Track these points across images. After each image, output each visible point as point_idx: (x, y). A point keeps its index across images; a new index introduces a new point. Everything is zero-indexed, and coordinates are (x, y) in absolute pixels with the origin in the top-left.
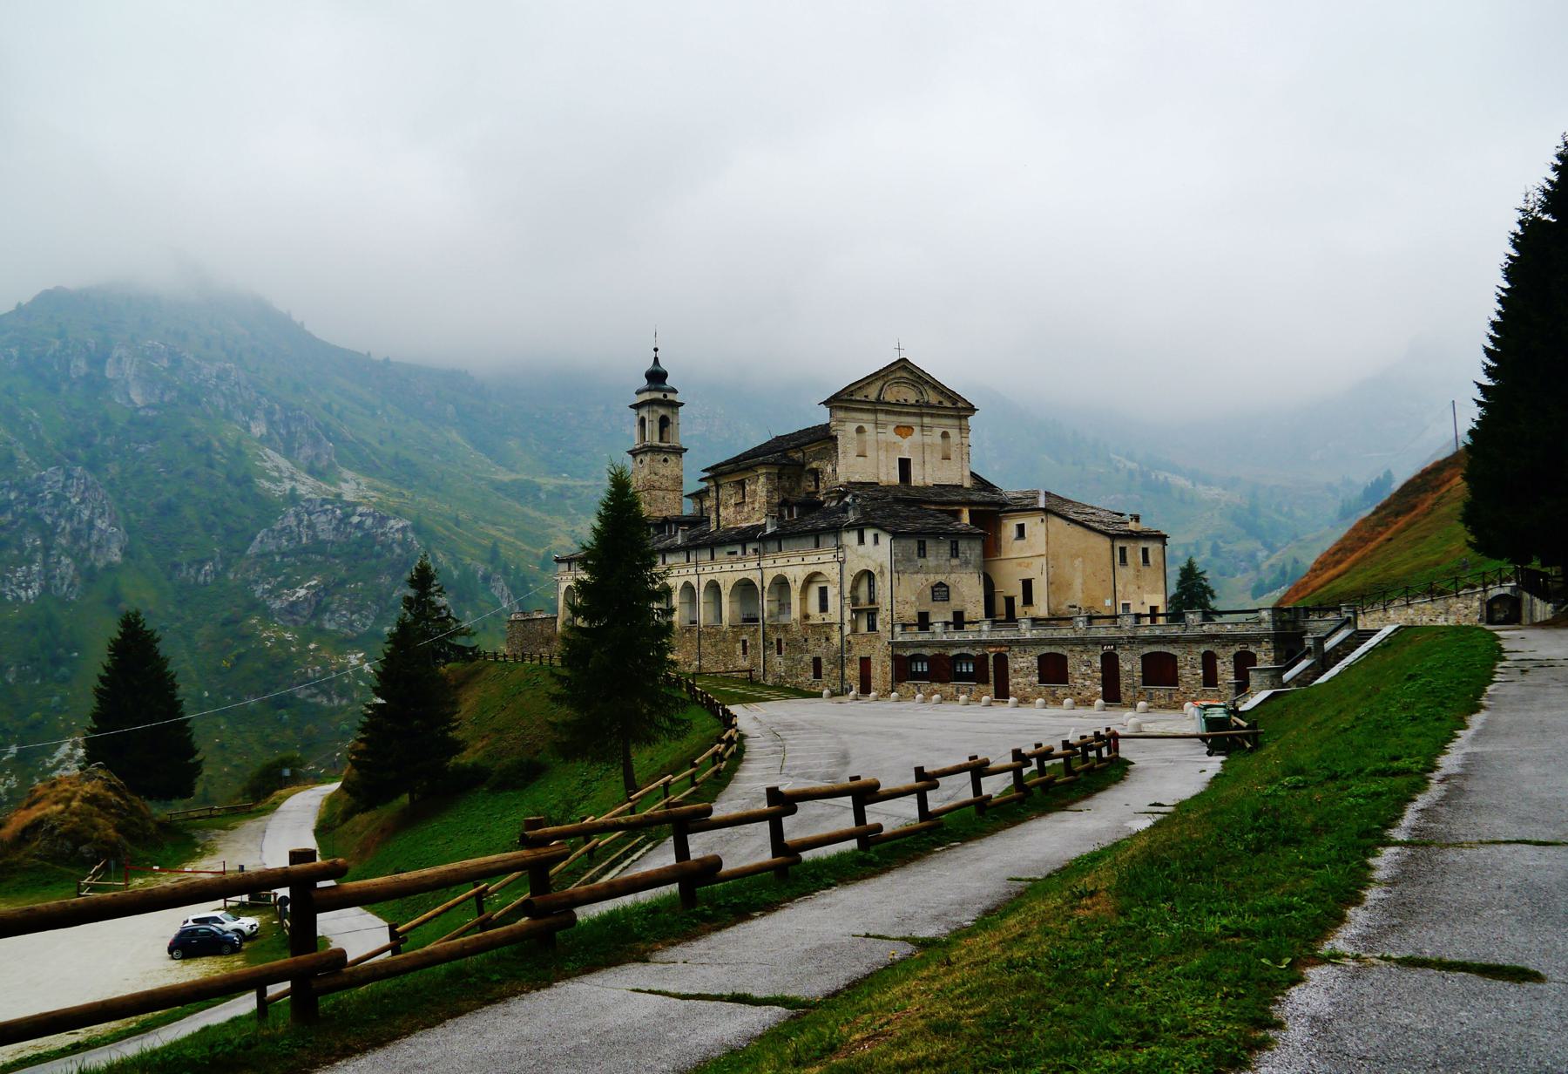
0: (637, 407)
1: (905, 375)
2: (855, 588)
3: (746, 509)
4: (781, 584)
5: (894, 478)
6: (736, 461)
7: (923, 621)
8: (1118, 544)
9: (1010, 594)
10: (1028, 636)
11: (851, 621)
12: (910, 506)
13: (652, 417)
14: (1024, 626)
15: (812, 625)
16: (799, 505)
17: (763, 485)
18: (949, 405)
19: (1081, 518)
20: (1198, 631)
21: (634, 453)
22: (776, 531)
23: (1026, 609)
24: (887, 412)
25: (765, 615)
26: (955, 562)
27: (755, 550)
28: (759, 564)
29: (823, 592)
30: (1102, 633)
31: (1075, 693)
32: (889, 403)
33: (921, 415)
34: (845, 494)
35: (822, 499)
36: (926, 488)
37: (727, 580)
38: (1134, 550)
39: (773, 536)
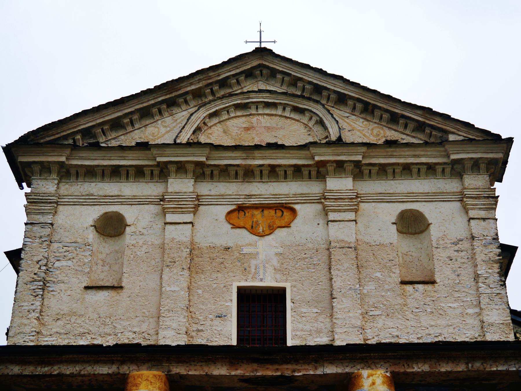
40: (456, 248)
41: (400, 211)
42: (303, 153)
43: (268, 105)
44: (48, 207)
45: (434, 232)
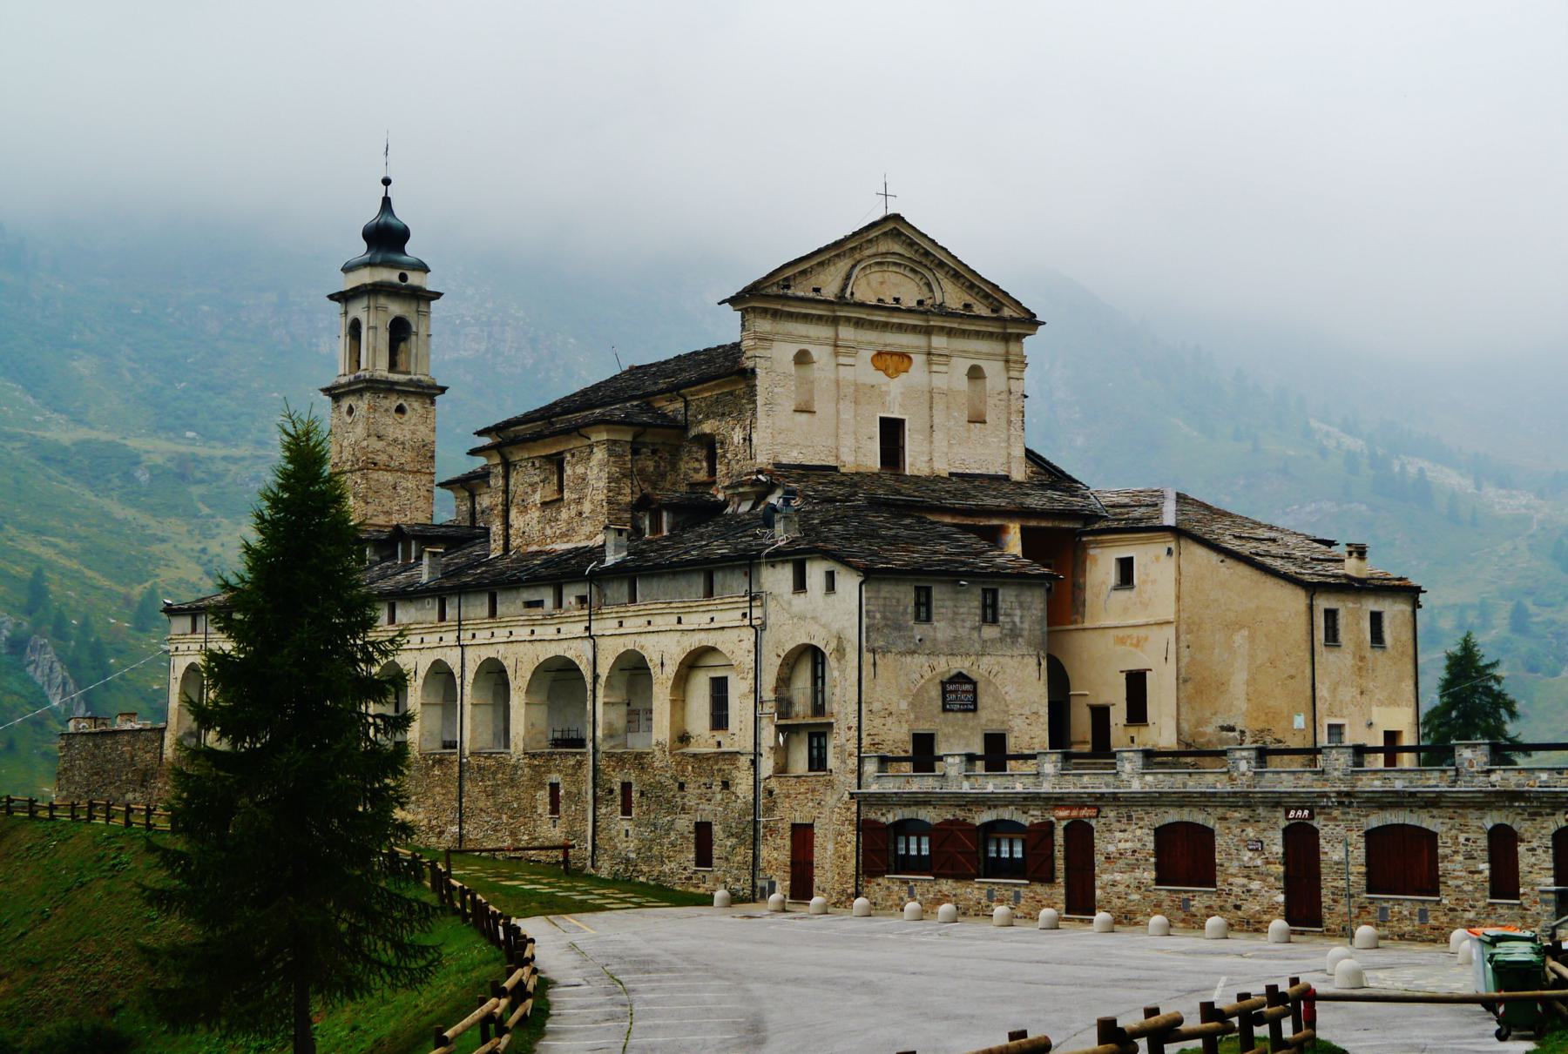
0: (344, 297)
1: (897, 248)
2: (784, 681)
3: (564, 515)
4: (634, 669)
5: (871, 459)
6: (546, 414)
7: (923, 753)
8: (1323, 603)
9: (1101, 700)
10: (1136, 786)
11: (776, 749)
12: (907, 516)
13: (375, 319)
14: (1128, 767)
15: (695, 755)
16: (673, 508)
17: (602, 466)
18: (985, 312)
19: (1247, 548)
20: (1480, 783)
21: (335, 393)
22: (624, 561)
23: (1133, 731)
24: (859, 323)
25: (599, 733)
26: (990, 632)
27: (582, 600)
28: (588, 629)
29: (719, 688)
30: (1286, 784)
31: (1229, 906)
32: (862, 305)
33: (928, 331)
34: (770, 488)
35: (721, 497)
36: (937, 479)
37: (522, 662)
38: (1354, 615)
39: (619, 571)
40: (1000, 397)
41: (969, 366)
42: (924, 317)
43: (895, 264)
44: (767, 344)
45: (988, 382)
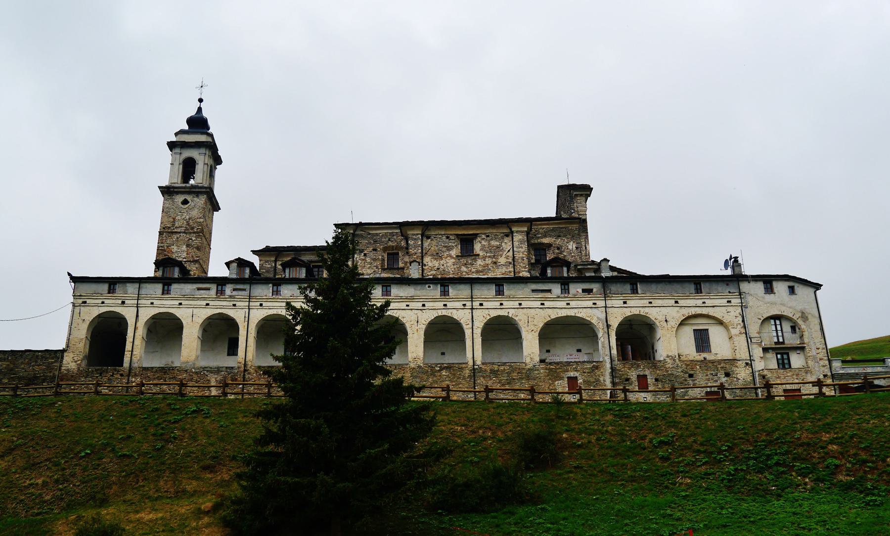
21: (167, 191)
